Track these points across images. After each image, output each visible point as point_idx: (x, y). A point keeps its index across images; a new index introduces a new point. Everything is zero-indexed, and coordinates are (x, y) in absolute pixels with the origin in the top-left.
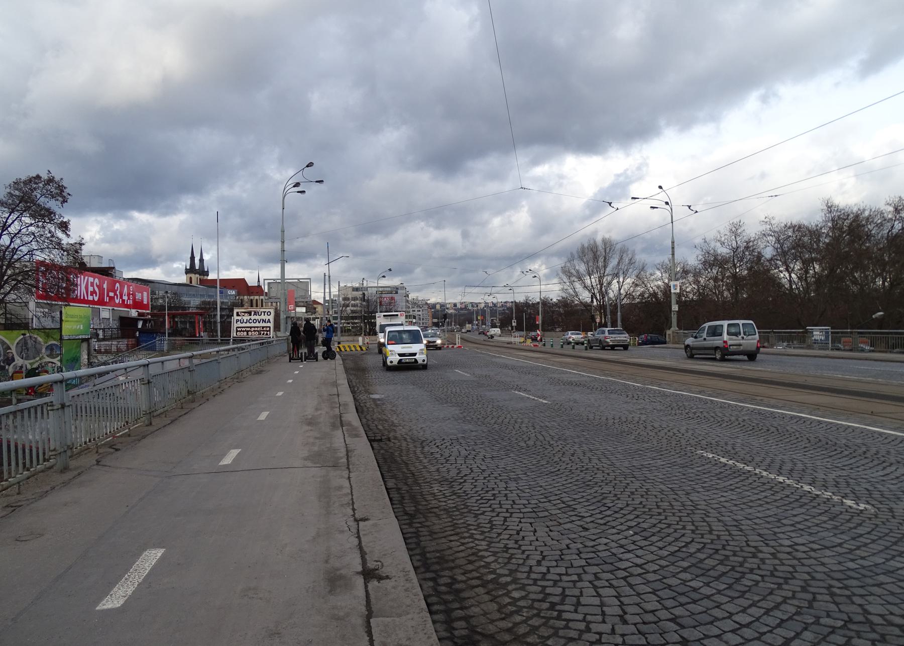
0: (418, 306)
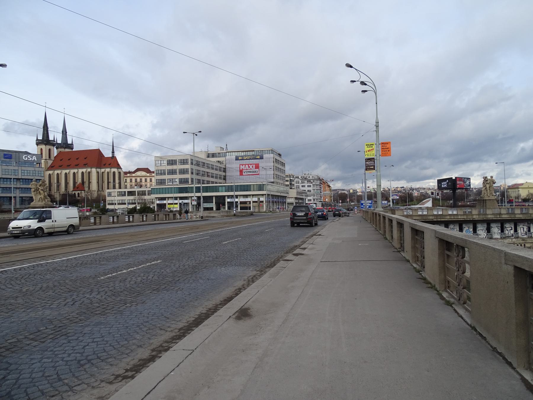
0: (309, 181)
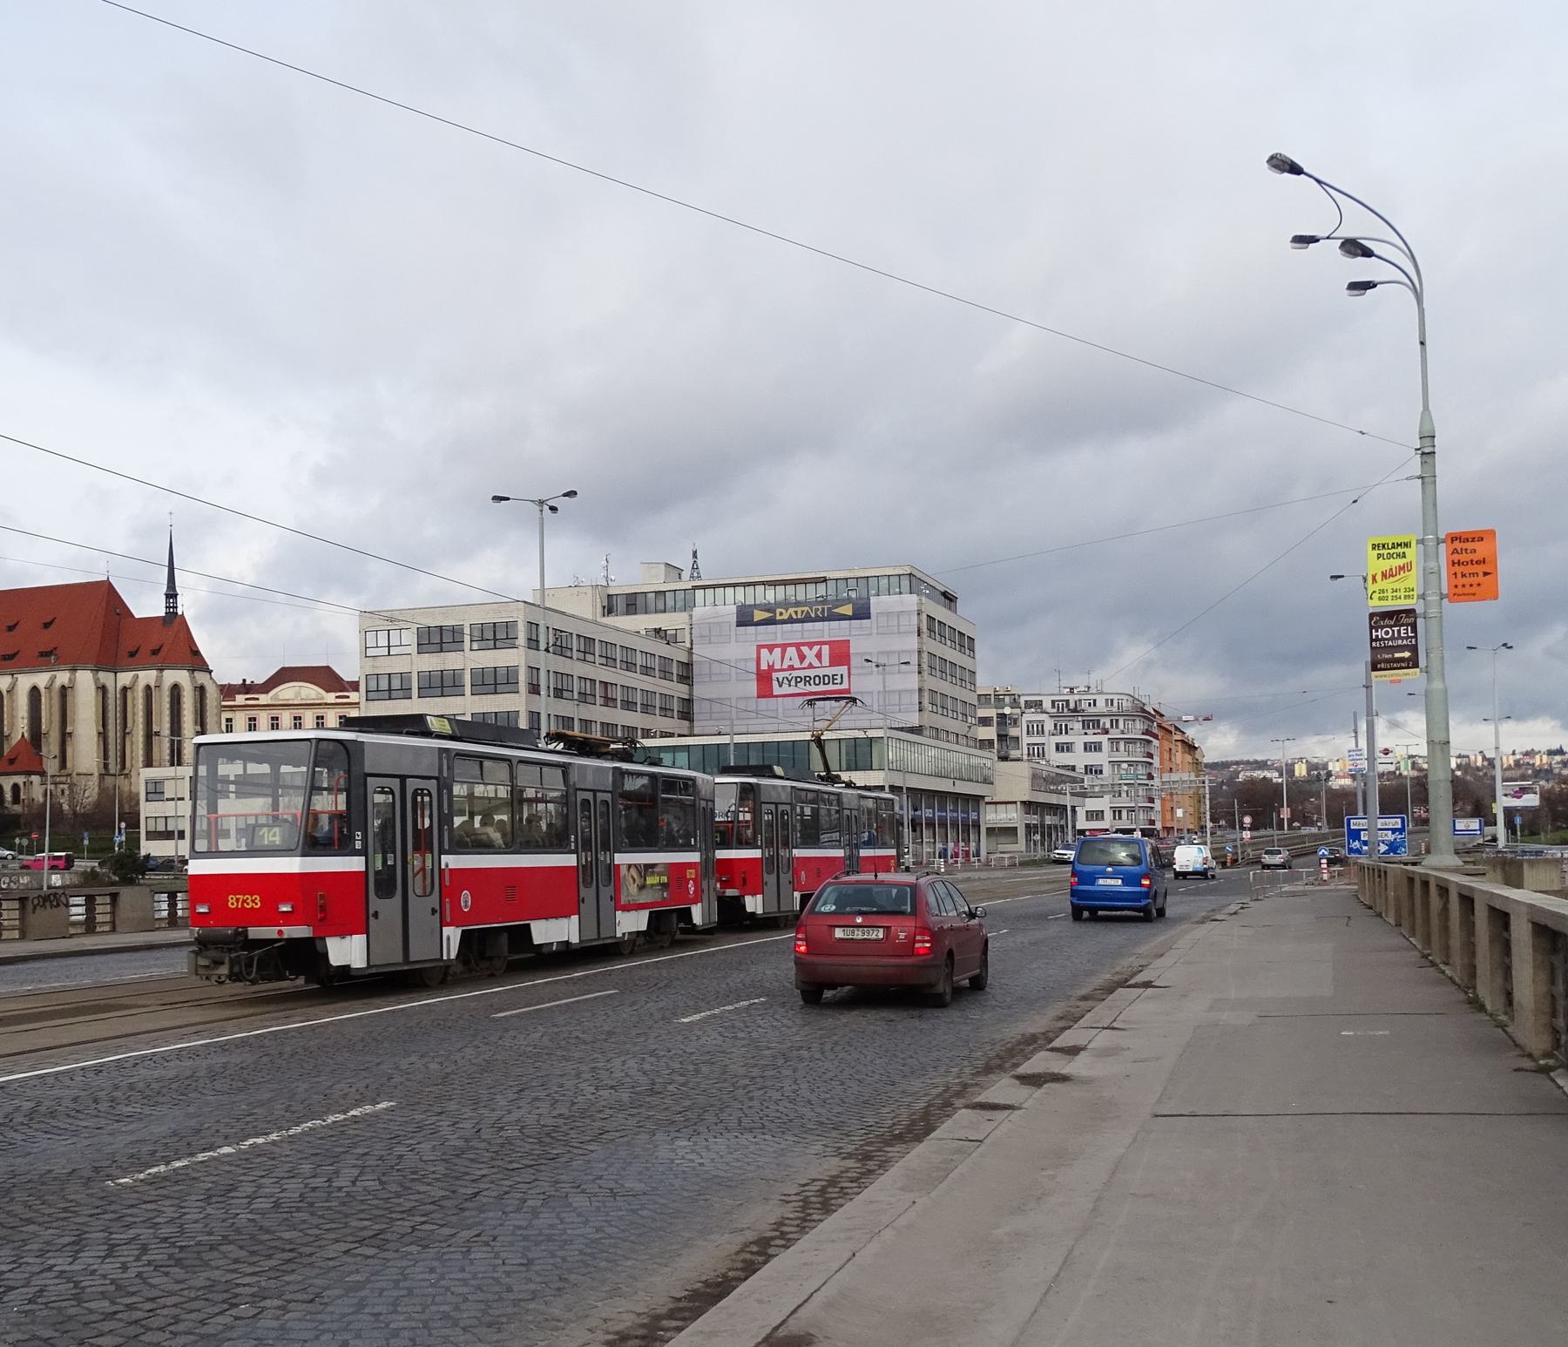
0: (1091, 723)
